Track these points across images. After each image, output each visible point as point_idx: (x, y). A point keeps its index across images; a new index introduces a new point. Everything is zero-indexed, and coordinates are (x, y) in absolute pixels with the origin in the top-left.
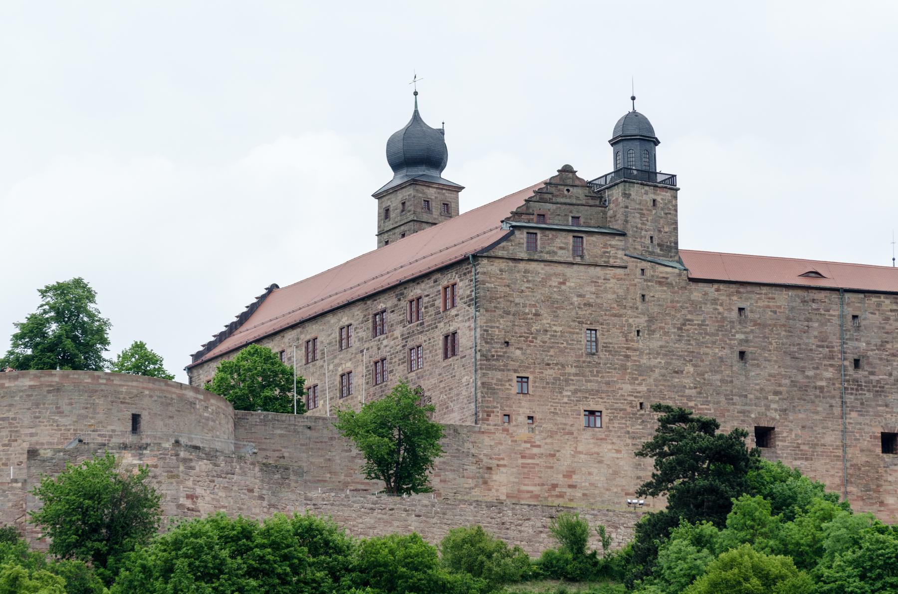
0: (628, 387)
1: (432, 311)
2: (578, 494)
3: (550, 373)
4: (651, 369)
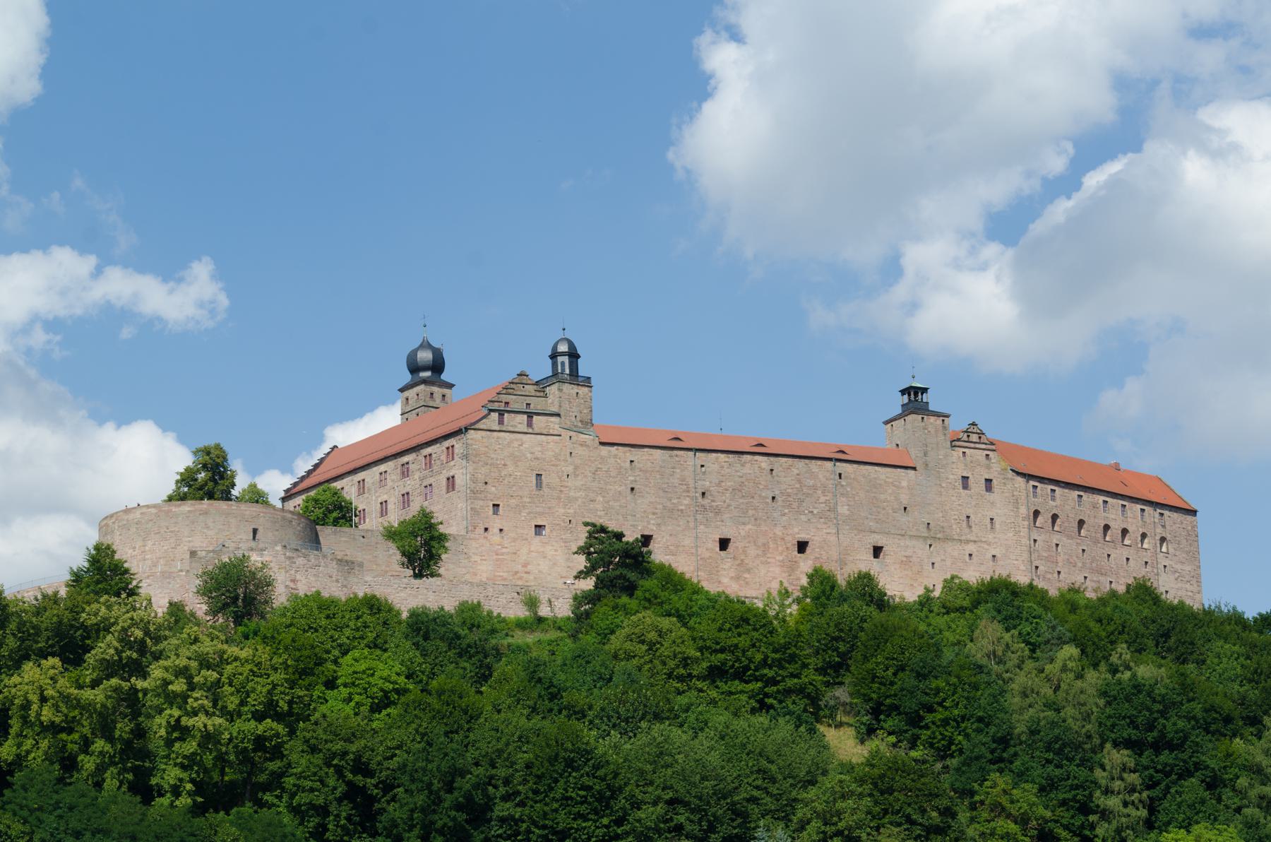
0: (562, 511)
1: (438, 462)
2: (531, 577)
3: (513, 502)
4: (576, 499)
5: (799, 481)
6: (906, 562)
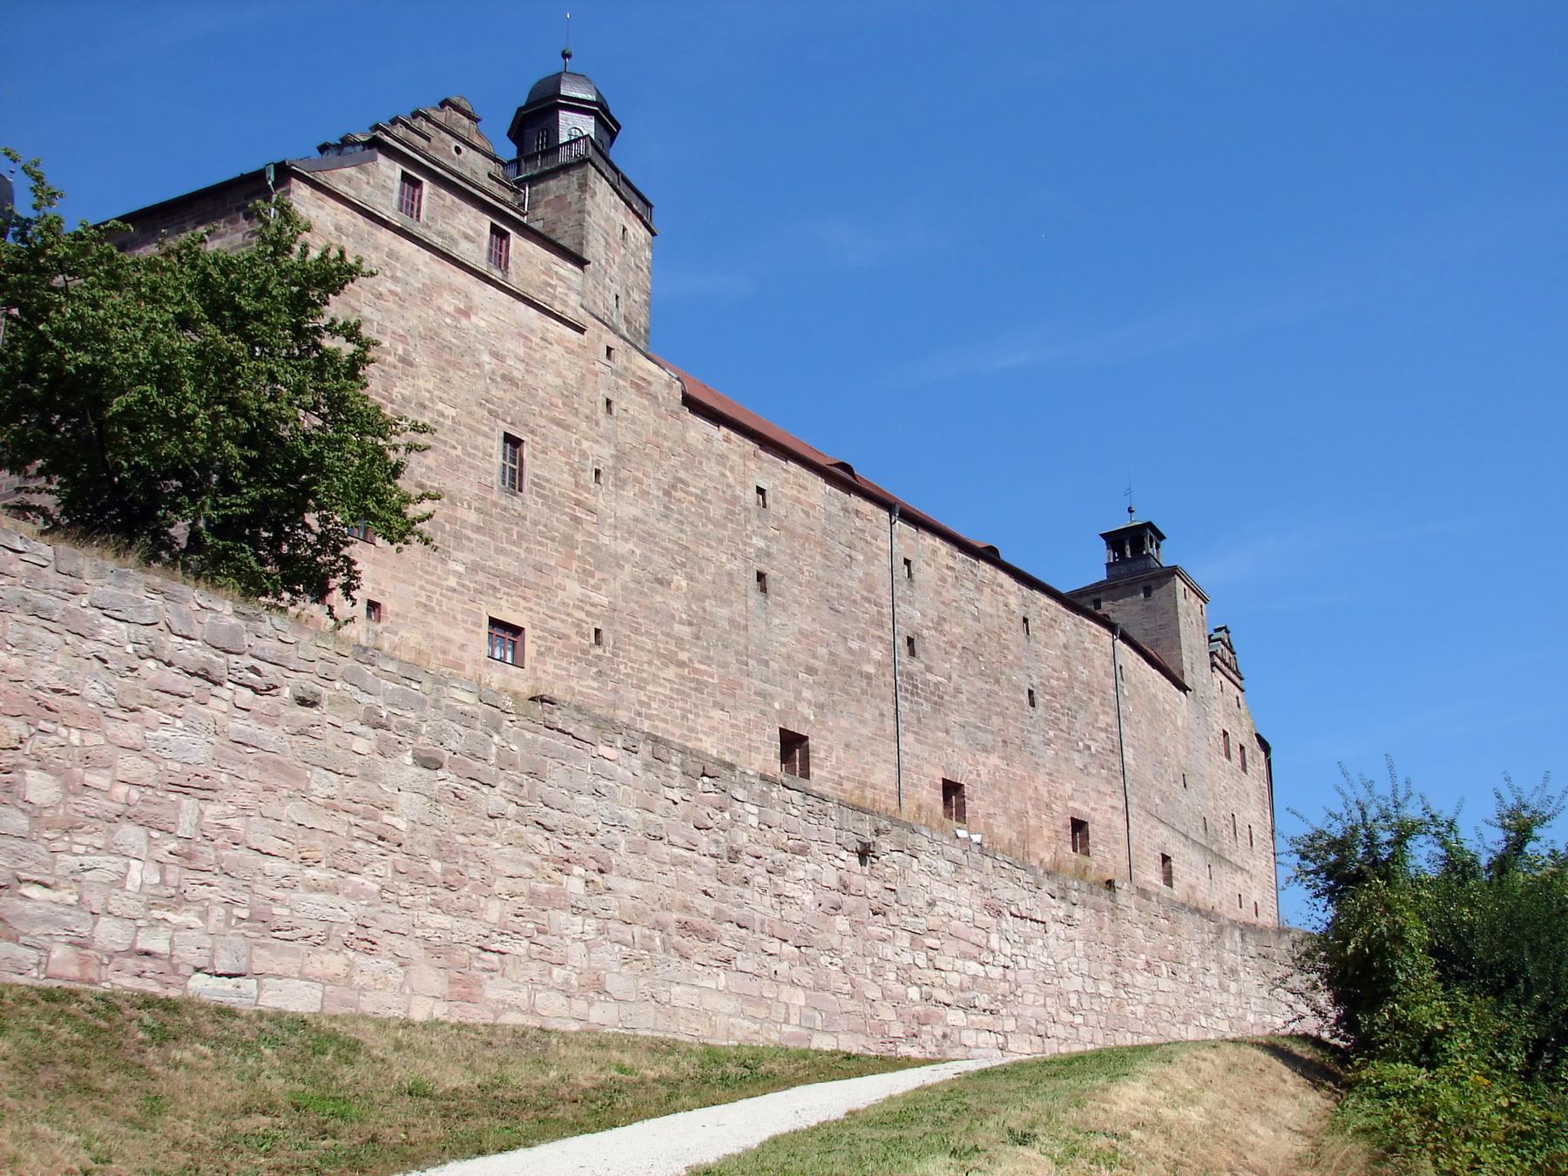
0: (574, 588)
4: (618, 561)
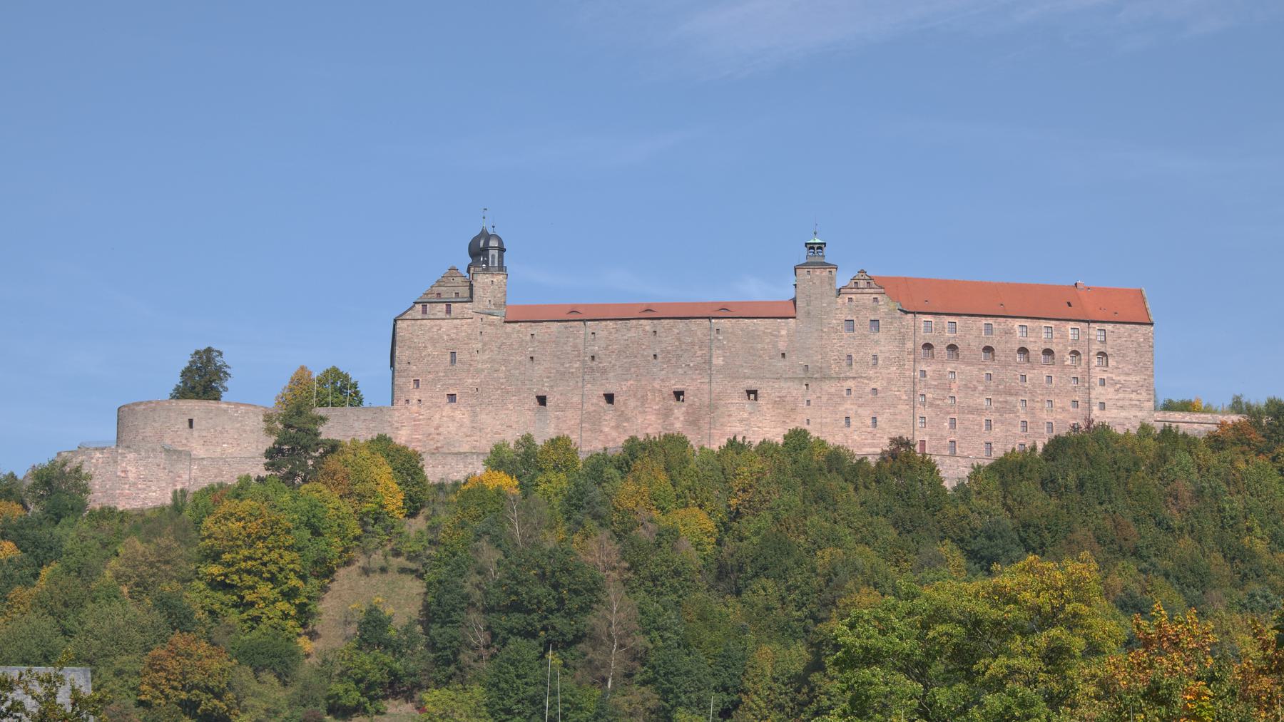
4: (483, 370)
5: (679, 339)
6: (780, 402)
